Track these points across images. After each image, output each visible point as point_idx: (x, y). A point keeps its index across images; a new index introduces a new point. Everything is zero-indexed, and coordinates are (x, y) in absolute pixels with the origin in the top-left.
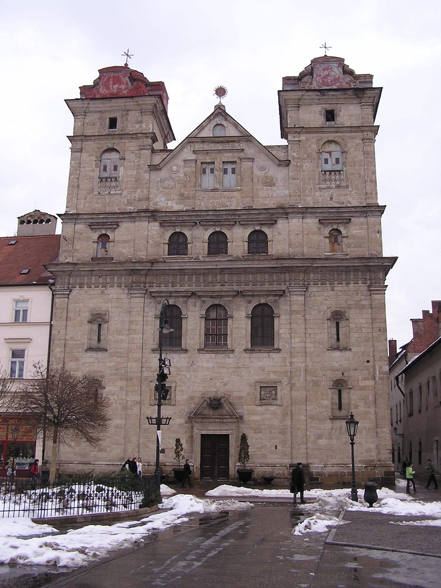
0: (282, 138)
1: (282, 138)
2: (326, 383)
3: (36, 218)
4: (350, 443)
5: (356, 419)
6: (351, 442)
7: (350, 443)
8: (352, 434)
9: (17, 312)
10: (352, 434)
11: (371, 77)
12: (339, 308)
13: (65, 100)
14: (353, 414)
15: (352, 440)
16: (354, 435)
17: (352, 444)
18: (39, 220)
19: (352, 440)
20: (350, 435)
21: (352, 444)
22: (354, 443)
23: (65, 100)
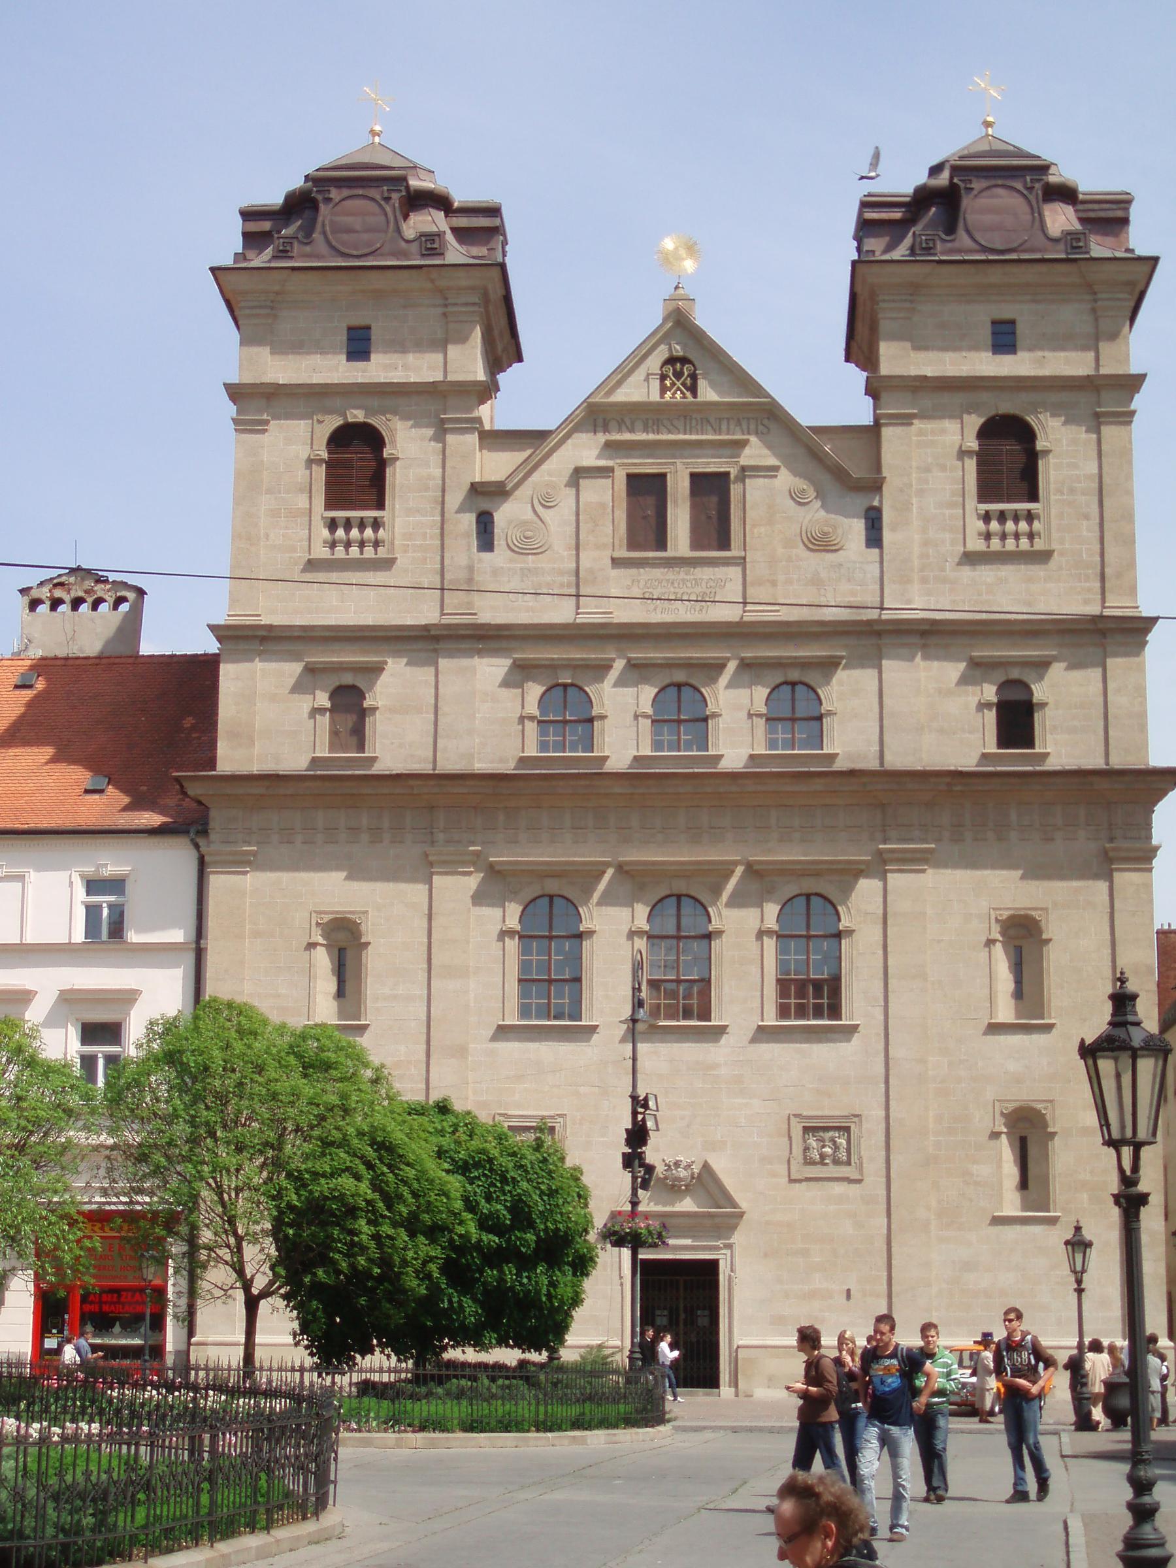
0: (847, 360)
1: (847, 360)
2: (985, 1119)
3: (81, 594)
4: (1075, 1290)
5: (1087, 1234)
6: (1076, 1286)
7: (1075, 1290)
8: (1079, 1268)
9: (92, 912)
10: (1079, 1268)
11: (1124, 202)
12: (1025, 909)
13: (213, 270)
14: (1081, 1225)
15: (1079, 1282)
16: (1083, 1271)
17: (1080, 1291)
18: (90, 600)
19: (1079, 1282)
20: (1074, 1272)
21: (1080, 1291)
22: (1083, 1290)
23: (213, 270)
